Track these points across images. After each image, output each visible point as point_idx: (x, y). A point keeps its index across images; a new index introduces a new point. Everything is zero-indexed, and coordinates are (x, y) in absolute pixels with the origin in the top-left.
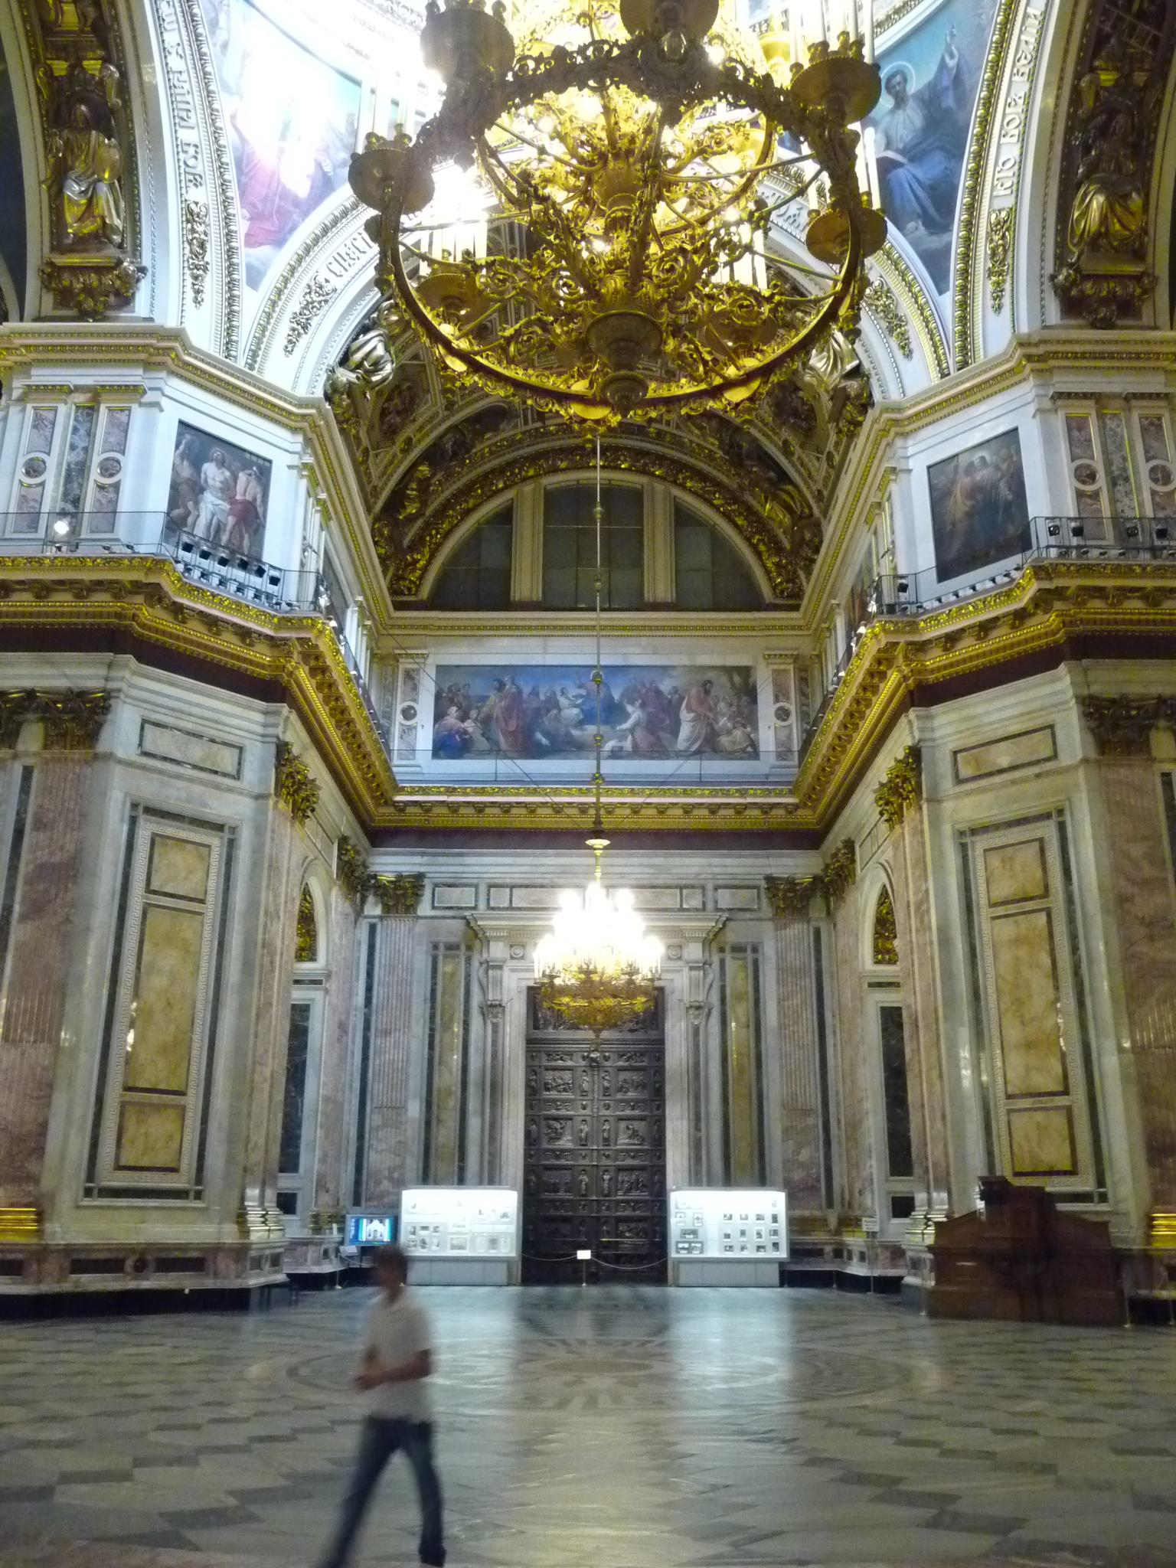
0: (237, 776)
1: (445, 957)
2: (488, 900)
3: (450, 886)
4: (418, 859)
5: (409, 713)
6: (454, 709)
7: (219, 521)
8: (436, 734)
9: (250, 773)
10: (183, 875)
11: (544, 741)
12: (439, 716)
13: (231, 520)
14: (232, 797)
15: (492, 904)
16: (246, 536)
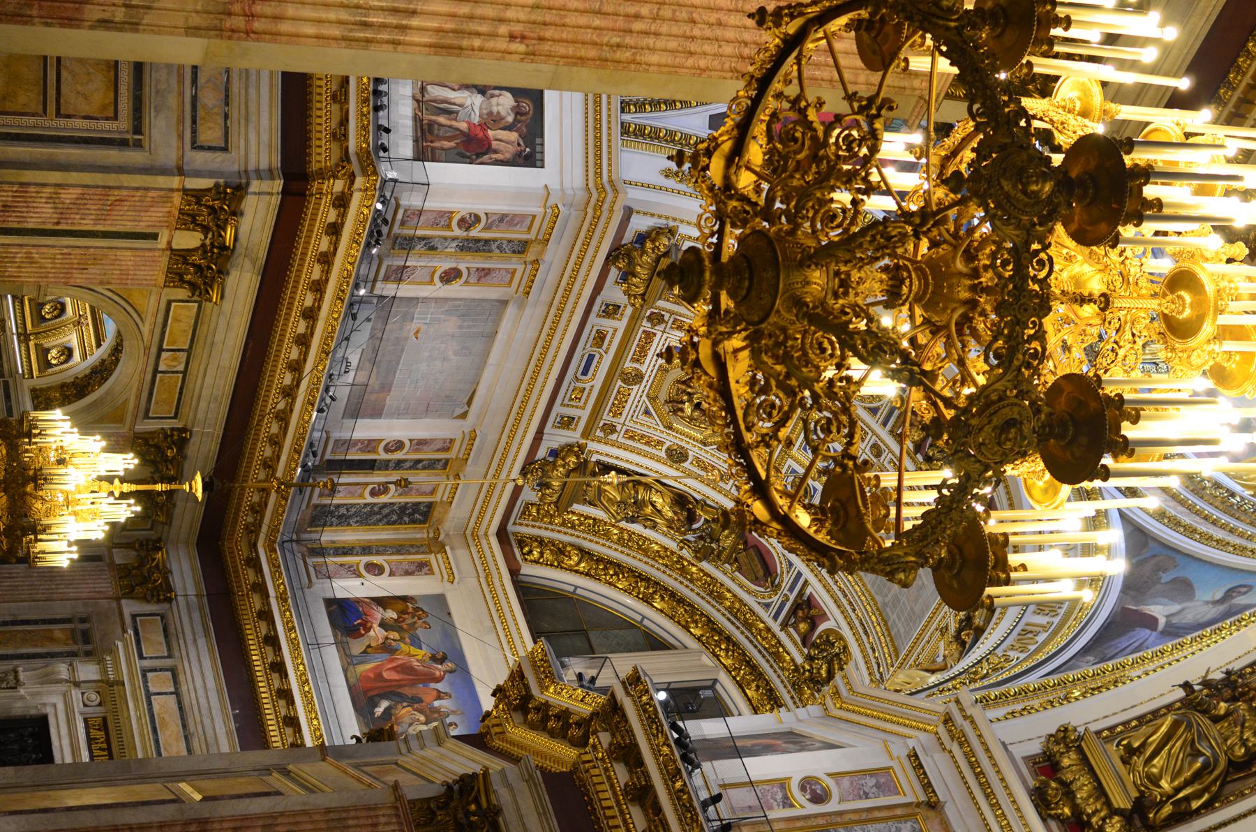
0: (196, 147)
1: (73, 631)
2: (155, 670)
3: (165, 630)
4: (191, 591)
5: (375, 569)
6: (395, 616)
7: (457, 113)
8: (358, 601)
9: (200, 159)
10: (80, 88)
11: (379, 711)
12: (382, 602)
13: (463, 126)
14: (174, 141)
15: (150, 675)
16: (452, 144)
